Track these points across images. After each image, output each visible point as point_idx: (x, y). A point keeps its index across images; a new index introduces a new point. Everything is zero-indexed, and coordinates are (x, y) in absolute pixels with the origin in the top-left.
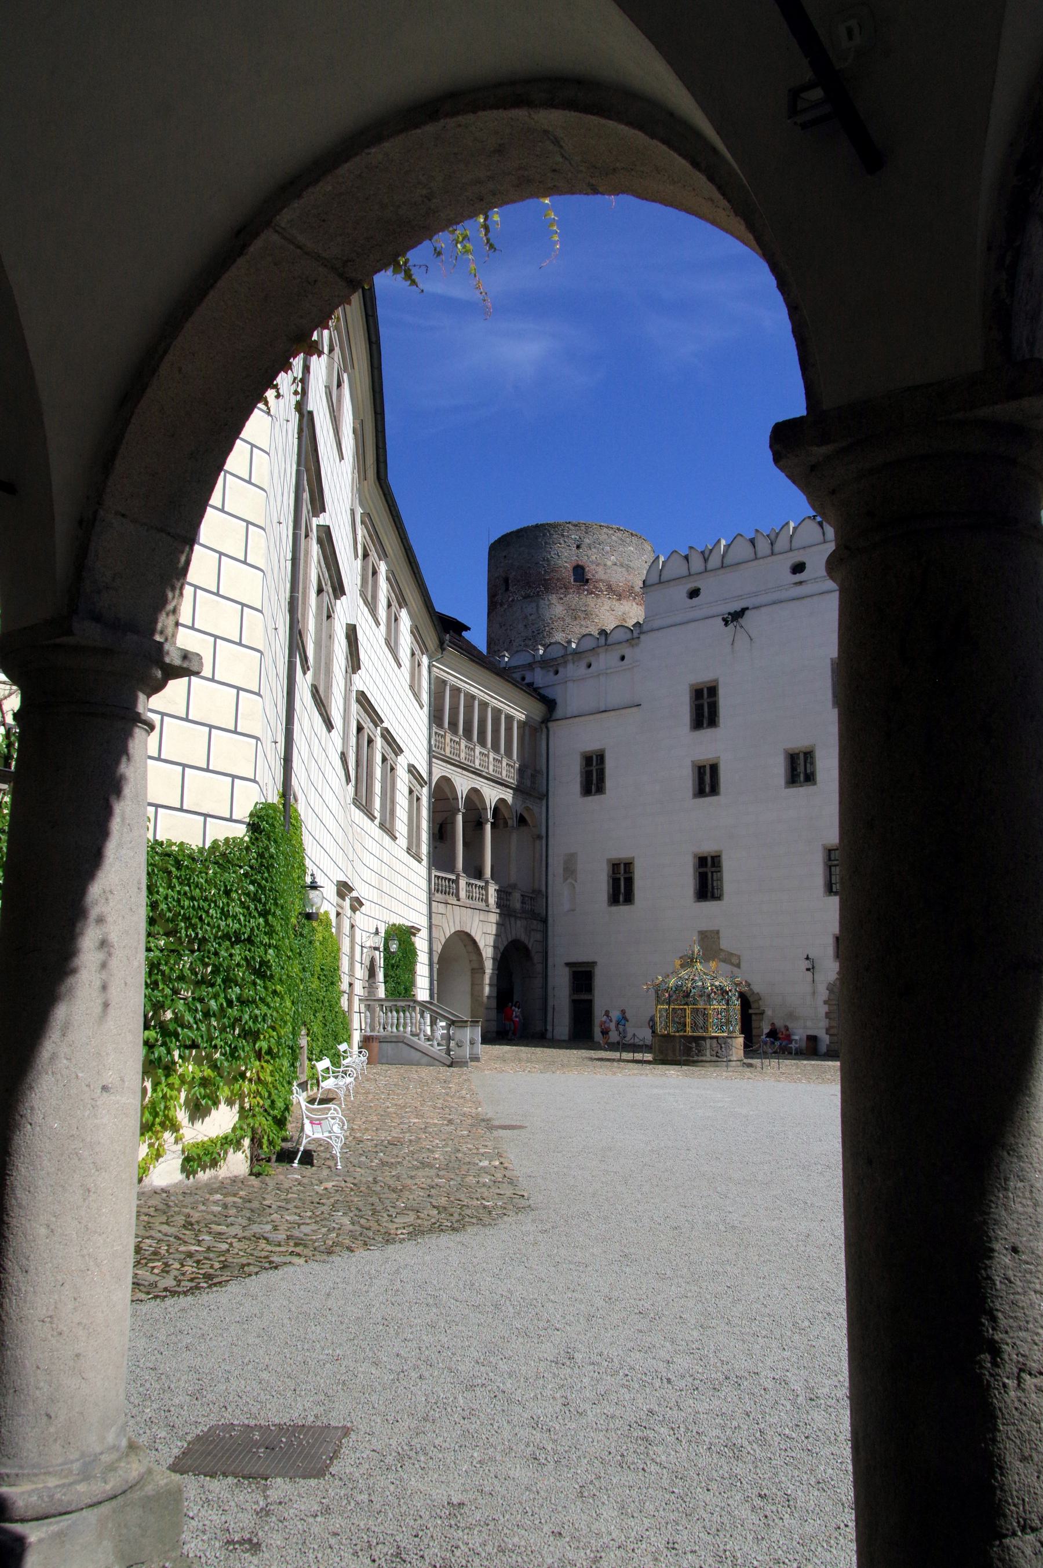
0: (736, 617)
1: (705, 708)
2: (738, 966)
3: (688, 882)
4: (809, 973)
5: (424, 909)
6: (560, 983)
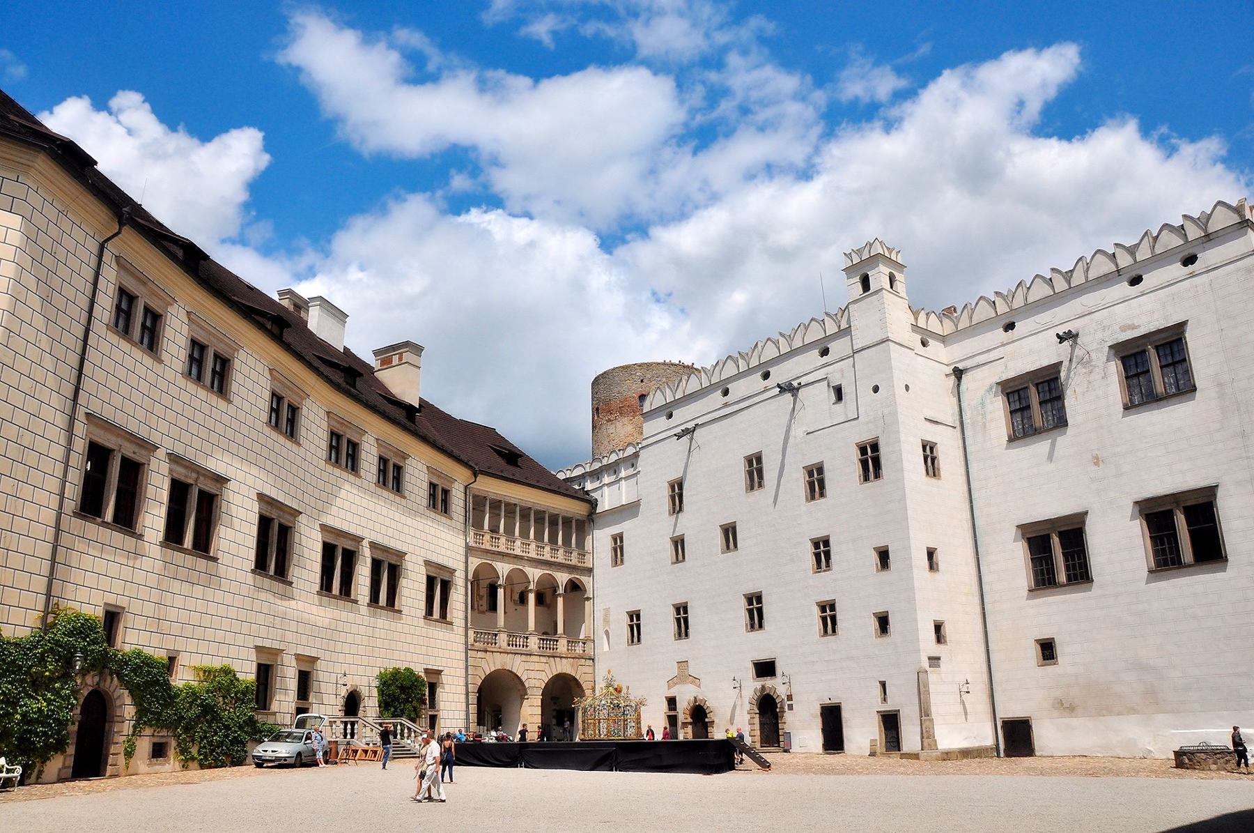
0: (686, 432)
4: (737, 690)
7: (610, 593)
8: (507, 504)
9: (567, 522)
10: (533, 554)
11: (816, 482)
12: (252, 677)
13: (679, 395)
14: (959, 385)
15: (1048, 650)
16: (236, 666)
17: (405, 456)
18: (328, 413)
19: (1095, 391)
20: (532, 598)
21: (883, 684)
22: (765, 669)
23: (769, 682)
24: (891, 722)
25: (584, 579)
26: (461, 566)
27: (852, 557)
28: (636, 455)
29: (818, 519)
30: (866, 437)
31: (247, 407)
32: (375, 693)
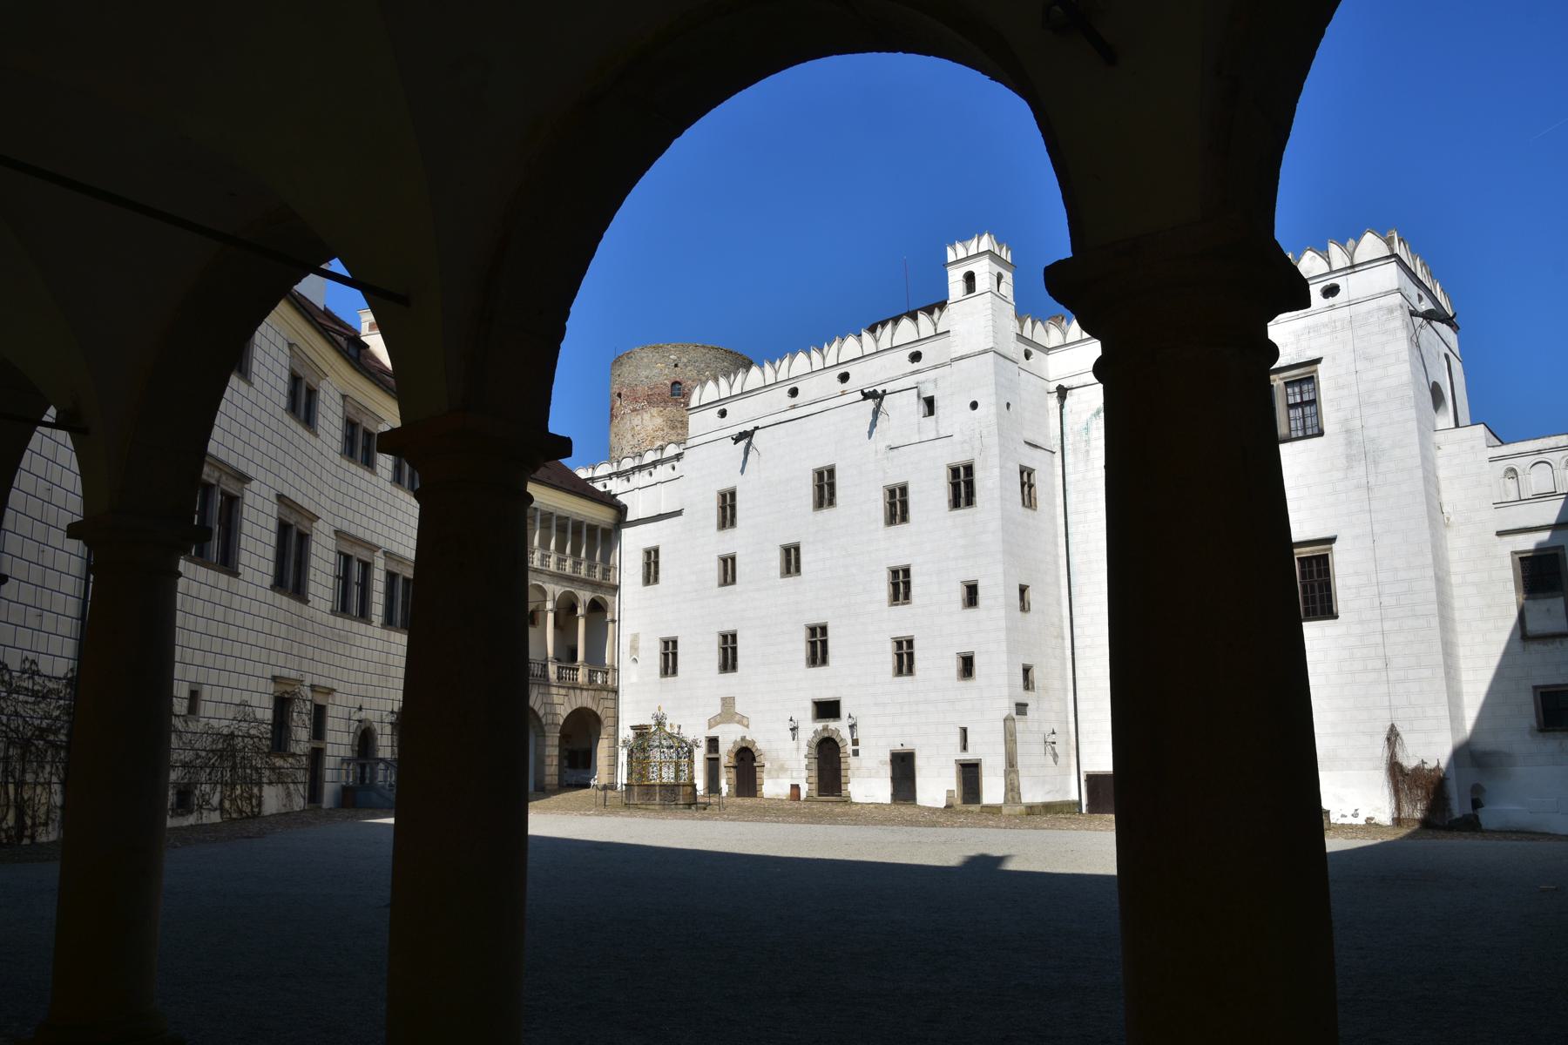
0: (745, 436)
7: (638, 618)
8: (559, 518)
9: (592, 529)
10: (553, 567)
11: (897, 506)
12: (268, 715)
13: (736, 390)
14: (1062, 407)
16: (255, 700)
18: (344, 397)
20: (550, 617)
21: (964, 730)
22: (827, 709)
24: (970, 774)
25: (608, 598)
27: (935, 589)
28: (678, 457)
29: (899, 545)
30: (960, 459)
31: (267, 389)
32: (388, 729)
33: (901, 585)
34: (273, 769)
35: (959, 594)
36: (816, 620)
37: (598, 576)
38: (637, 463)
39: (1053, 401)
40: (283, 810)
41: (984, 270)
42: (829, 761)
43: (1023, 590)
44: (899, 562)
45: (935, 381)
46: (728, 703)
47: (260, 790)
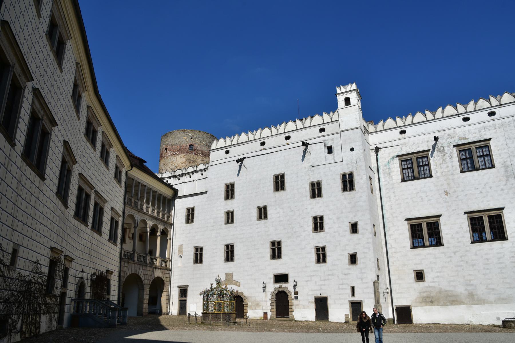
0: (240, 161)
1: (230, 192)
2: (239, 286)
3: (222, 255)
5: (117, 264)
6: (175, 293)
9: (165, 198)
11: (316, 190)
13: (234, 142)
15: (420, 276)
17: (111, 146)
19: (445, 165)
21: (353, 288)
22: (281, 278)
23: (284, 285)
25: (169, 229)
26: (121, 213)
28: (205, 170)
29: (317, 208)
30: (347, 171)
33: (318, 224)
34: (46, 304)
35: (348, 228)
36: (275, 239)
37: (166, 219)
38: (184, 172)
39: (373, 153)
40: (48, 331)
41: (354, 98)
42: (282, 303)
43: (374, 226)
44: (318, 214)
45: (333, 140)
46: (229, 276)
47: (40, 318)
